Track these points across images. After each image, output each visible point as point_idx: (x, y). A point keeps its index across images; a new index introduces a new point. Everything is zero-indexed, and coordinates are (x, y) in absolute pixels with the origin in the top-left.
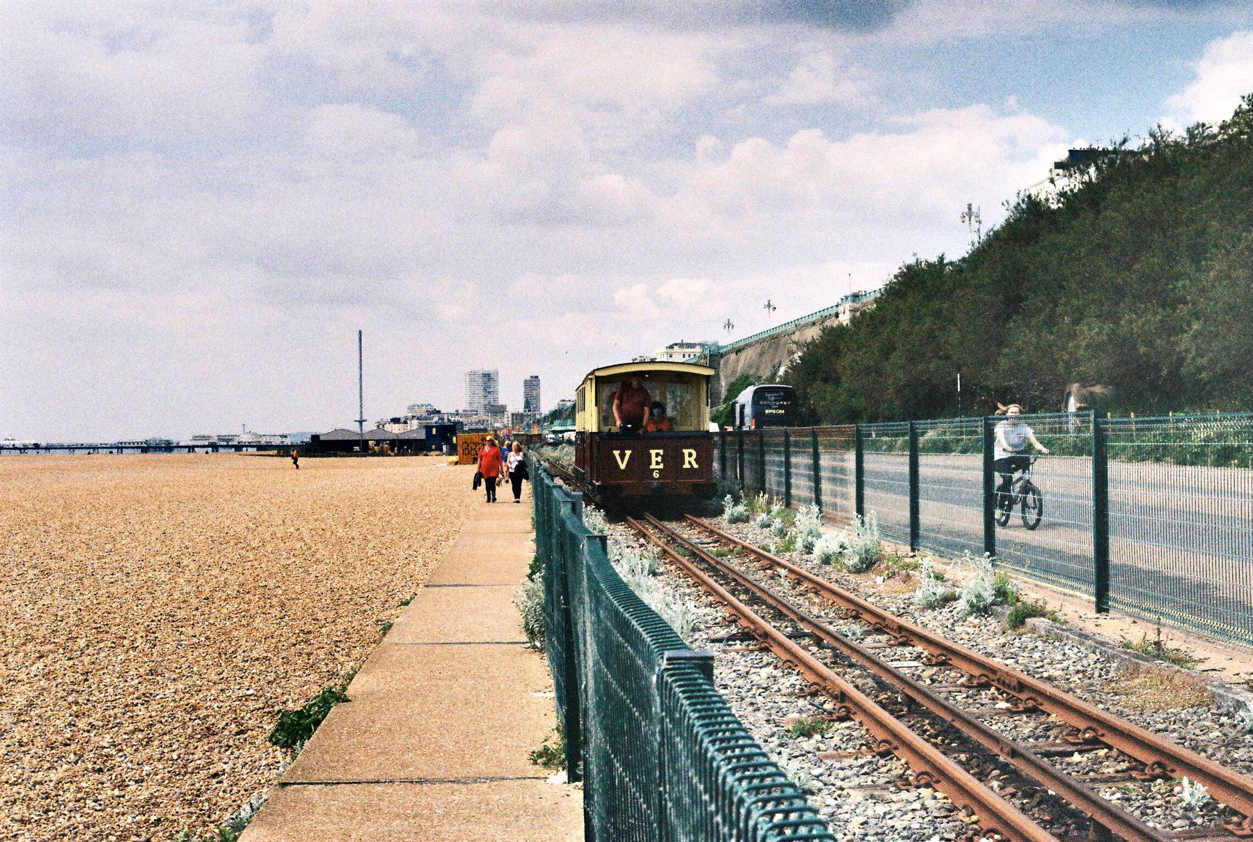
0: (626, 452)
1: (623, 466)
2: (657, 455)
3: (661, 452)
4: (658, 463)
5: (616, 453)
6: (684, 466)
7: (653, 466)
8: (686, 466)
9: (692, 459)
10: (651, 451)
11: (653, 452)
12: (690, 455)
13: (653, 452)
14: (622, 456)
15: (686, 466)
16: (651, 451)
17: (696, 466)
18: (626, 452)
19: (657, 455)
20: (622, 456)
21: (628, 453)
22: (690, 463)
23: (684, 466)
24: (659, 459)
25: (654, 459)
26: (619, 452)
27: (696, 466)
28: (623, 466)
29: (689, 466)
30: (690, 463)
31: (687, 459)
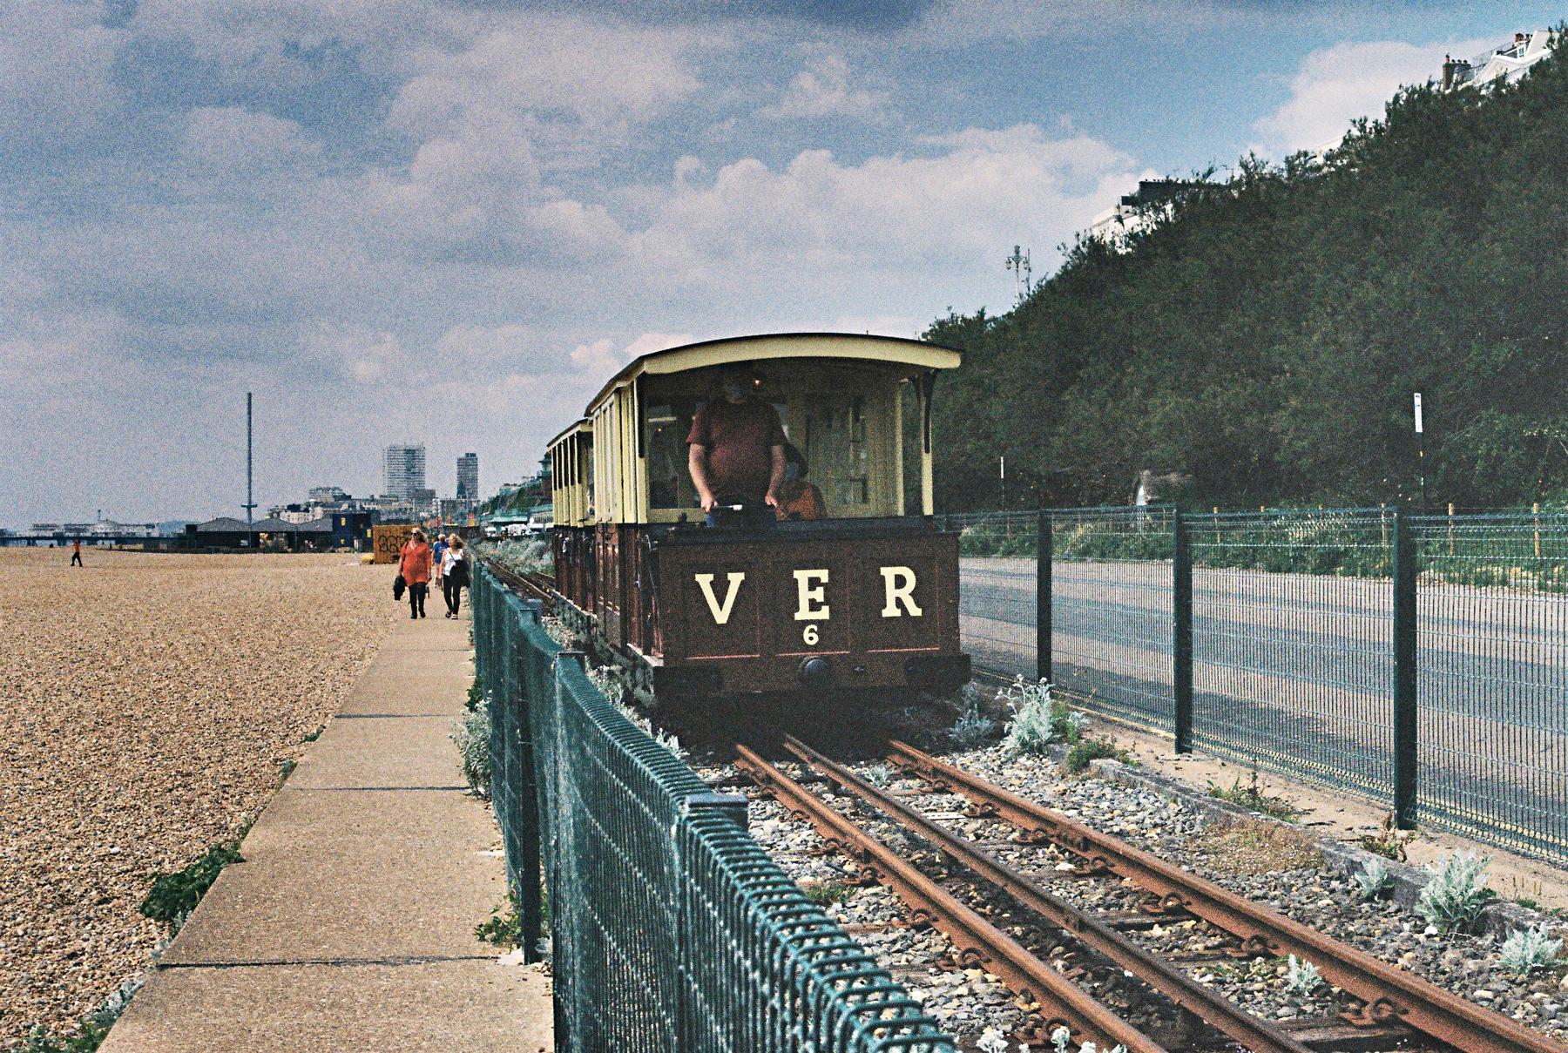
0: (731, 576)
1: (721, 616)
2: (814, 583)
3: (824, 575)
4: (814, 606)
5: (704, 580)
6: (886, 613)
7: (803, 614)
8: (891, 611)
9: (905, 594)
10: (797, 574)
11: (802, 576)
12: (900, 582)
13: (802, 576)
14: (720, 589)
15: (891, 611)
16: (797, 574)
17: (915, 611)
18: (731, 576)
19: (814, 583)
20: (720, 589)
21: (736, 579)
22: (899, 603)
23: (886, 613)
24: (819, 595)
25: (804, 596)
26: (710, 577)
27: (915, 611)
28: (721, 616)
29: (897, 613)
30: (899, 603)
31: (891, 593)
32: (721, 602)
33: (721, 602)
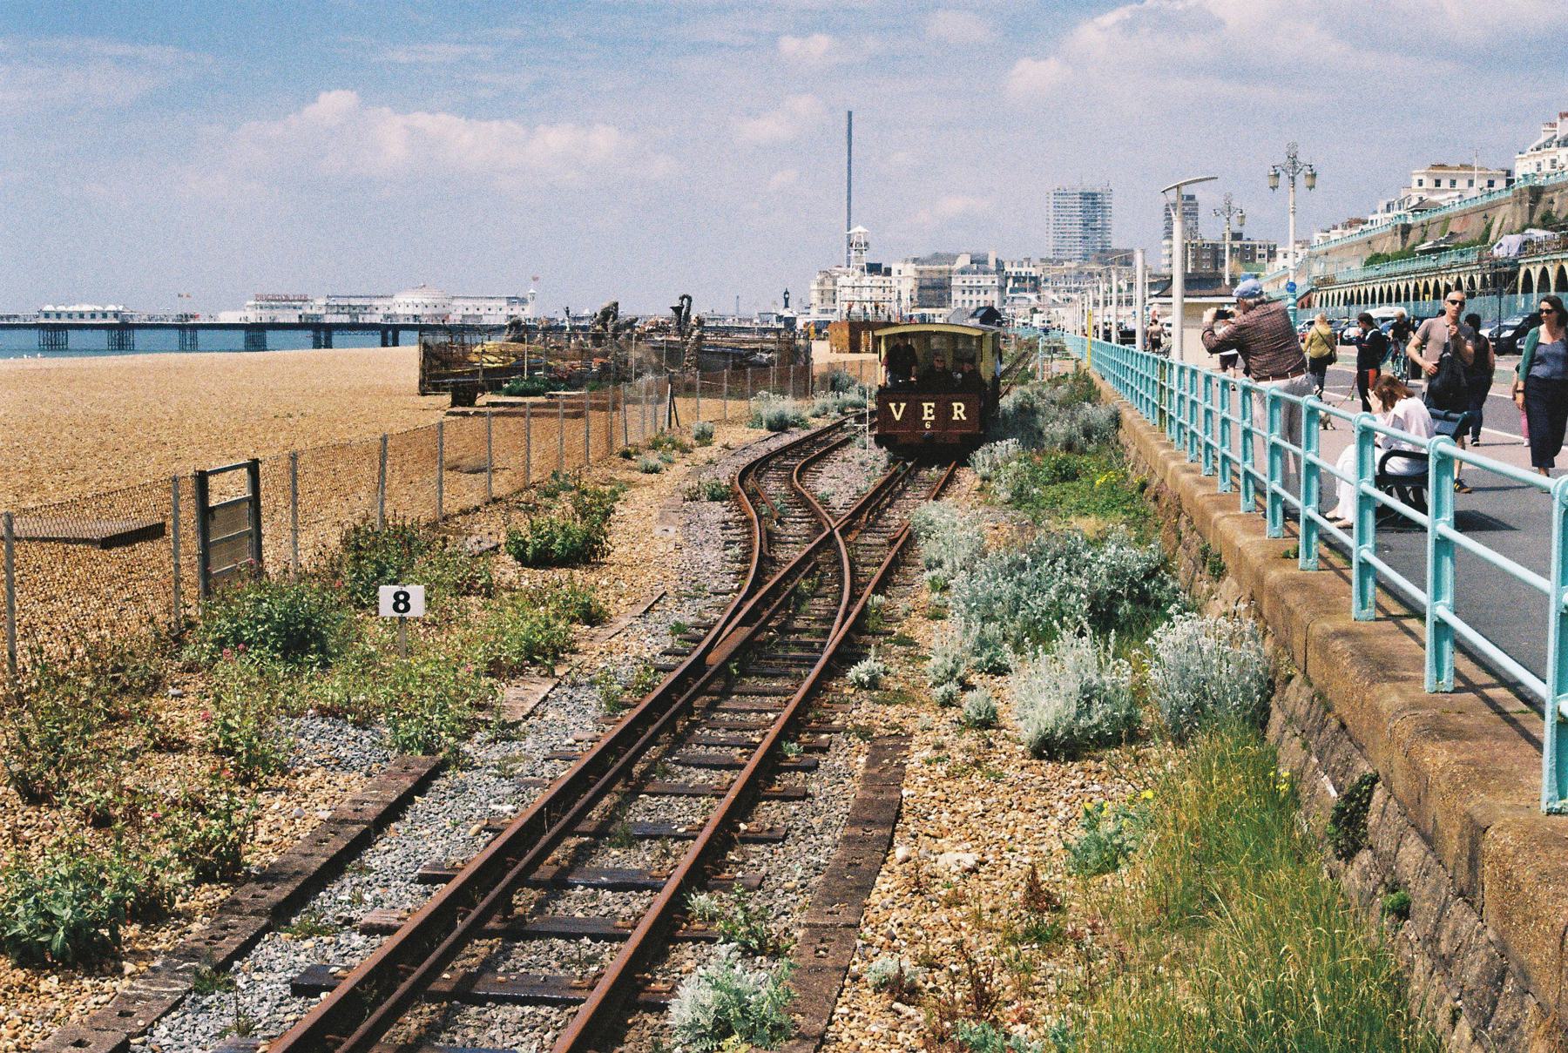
1: (898, 417)
2: (929, 408)
3: (933, 405)
4: (930, 415)
5: (892, 405)
7: (925, 418)
8: (955, 418)
9: (961, 412)
11: (925, 405)
12: (959, 408)
13: (925, 405)
14: (898, 408)
15: (955, 418)
17: (964, 418)
19: (929, 408)
20: (898, 408)
21: (903, 405)
24: (931, 411)
25: (926, 411)
27: (964, 418)
28: (898, 417)
31: (956, 412)
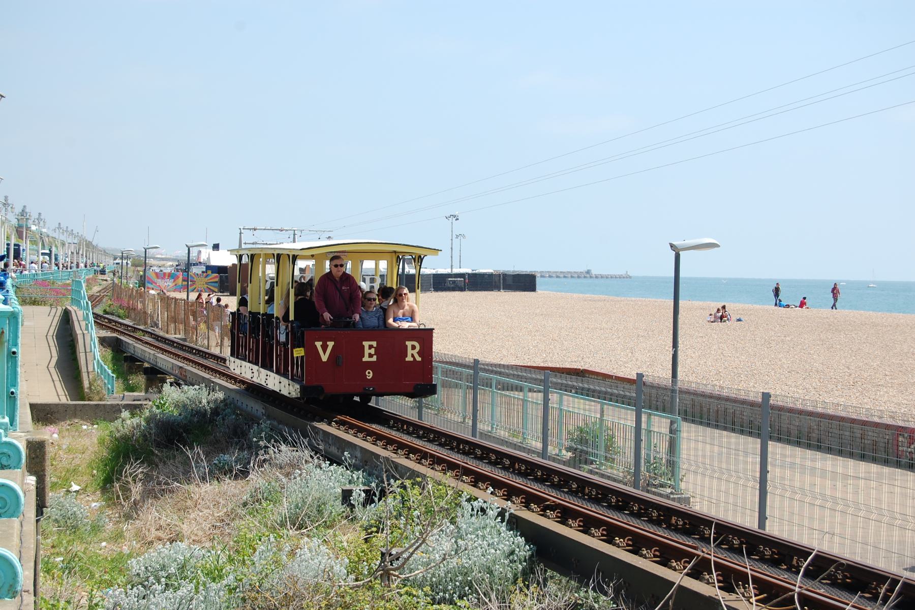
0: (328, 343)
1: (325, 358)
2: (371, 347)
3: (374, 344)
4: (370, 356)
5: (318, 344)
6: (407, 359)
7: (366, 359)
8: (409, 358)
9: (415, 352)
10: (364, 343)
11: (366, 344)
12: (413, 347)
13: (366, 344)
14: (325, 348)
15: (409, 358)
16: (364, 343)
17: (419, 359)
18: (328, 343)
19: (371, 347)
20: (325, 348)
21: (331, 344)
22: (413, 356)
23: (407, 359)
24: (372, 351)
25: (367, 351)
26: (321, 343)
27: (419, 359)
28: (325, 358)
29: (412, 359)
30: (413, 356)
31: (410, 351)
32: (324, 353)
33: (324, 353)
